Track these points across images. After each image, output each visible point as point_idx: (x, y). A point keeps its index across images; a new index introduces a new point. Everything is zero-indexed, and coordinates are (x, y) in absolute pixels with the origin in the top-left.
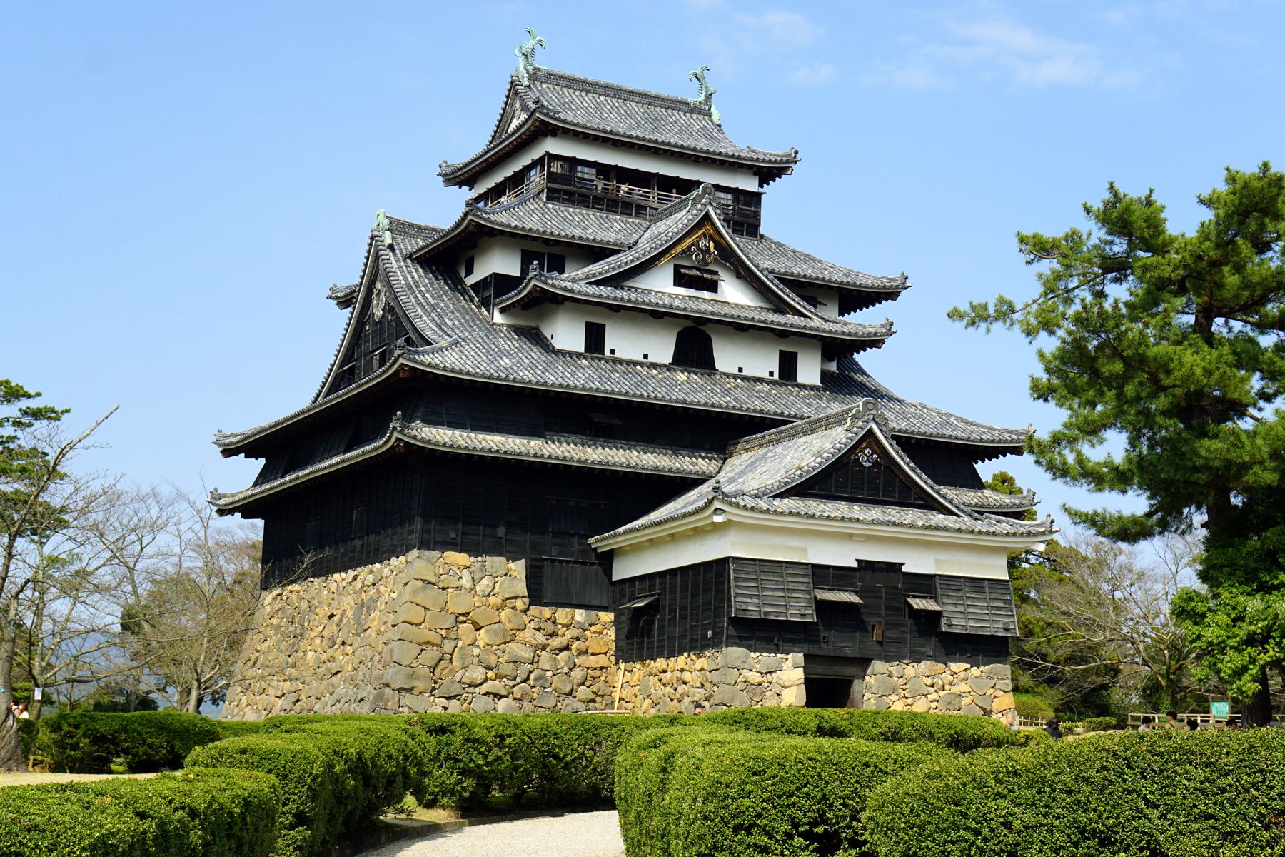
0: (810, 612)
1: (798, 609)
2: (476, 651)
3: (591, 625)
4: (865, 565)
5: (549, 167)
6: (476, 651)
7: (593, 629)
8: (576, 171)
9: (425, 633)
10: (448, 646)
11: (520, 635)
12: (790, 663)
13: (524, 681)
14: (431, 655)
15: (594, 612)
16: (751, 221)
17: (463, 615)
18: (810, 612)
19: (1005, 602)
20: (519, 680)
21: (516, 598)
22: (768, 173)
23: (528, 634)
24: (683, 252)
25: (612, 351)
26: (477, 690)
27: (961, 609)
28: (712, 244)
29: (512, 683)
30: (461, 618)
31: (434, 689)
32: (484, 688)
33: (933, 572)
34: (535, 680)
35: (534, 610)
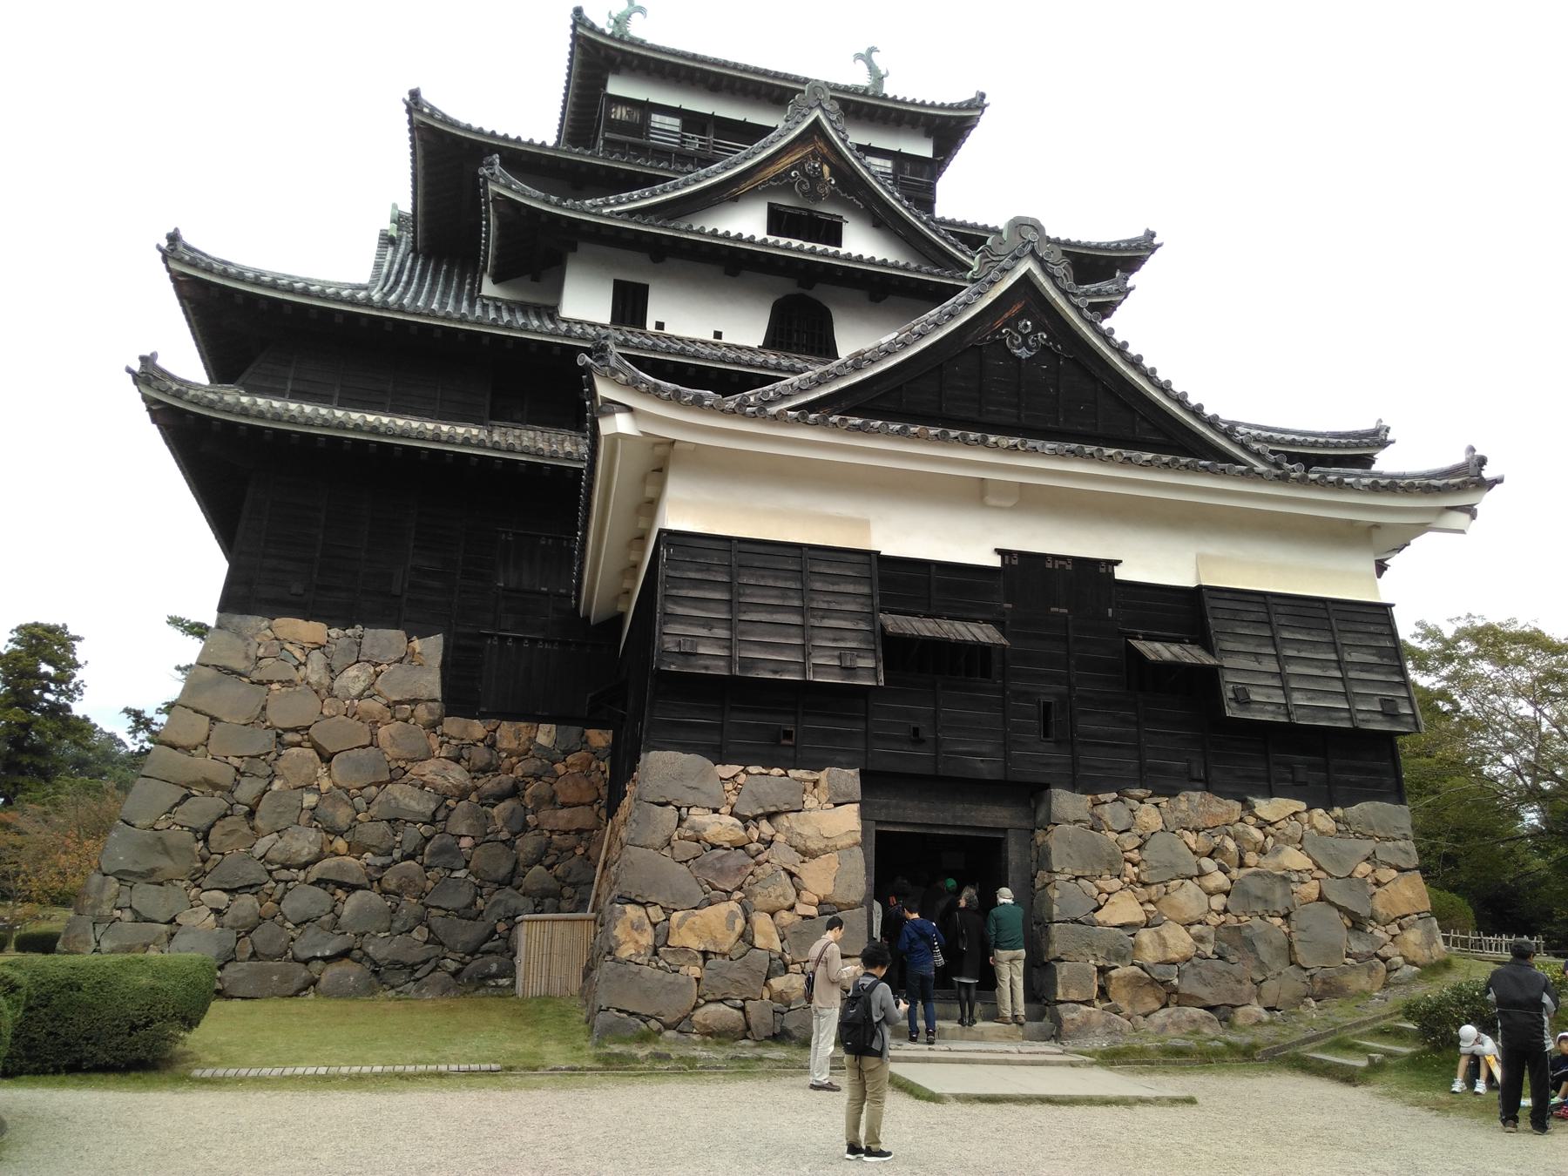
0: (869, 663)
1: (838, 654)
2: (310, 799)
3: (567, 753)
4: (1020, 565)
5: (608, 113)
6: (310, 799)
7: (570, 759)
8: (646, 119)
9: (203, 765)
10: (247, 790)
11: (415, 769)
12: (823, 794)
13: (411, 857)
14: (204, 807)
15: (574, 730)
16: (921, 195)
17: (295, 730)
18: (868, 663)
19: (1380, 651)
20: (397, 854)
21: (415, 701)
22: (949, 129)
23: (429, 769)
24: (777, 177)
25: (660, 326)
26: (302, 875)
27: (1274, 668)
28: (826, 169)
29: (379, 861)
30: (289, 737)
31: (205, 874)
32: (315, 872)
33: (1192, 584)
34: (433, 854)
35: (453, 725)
